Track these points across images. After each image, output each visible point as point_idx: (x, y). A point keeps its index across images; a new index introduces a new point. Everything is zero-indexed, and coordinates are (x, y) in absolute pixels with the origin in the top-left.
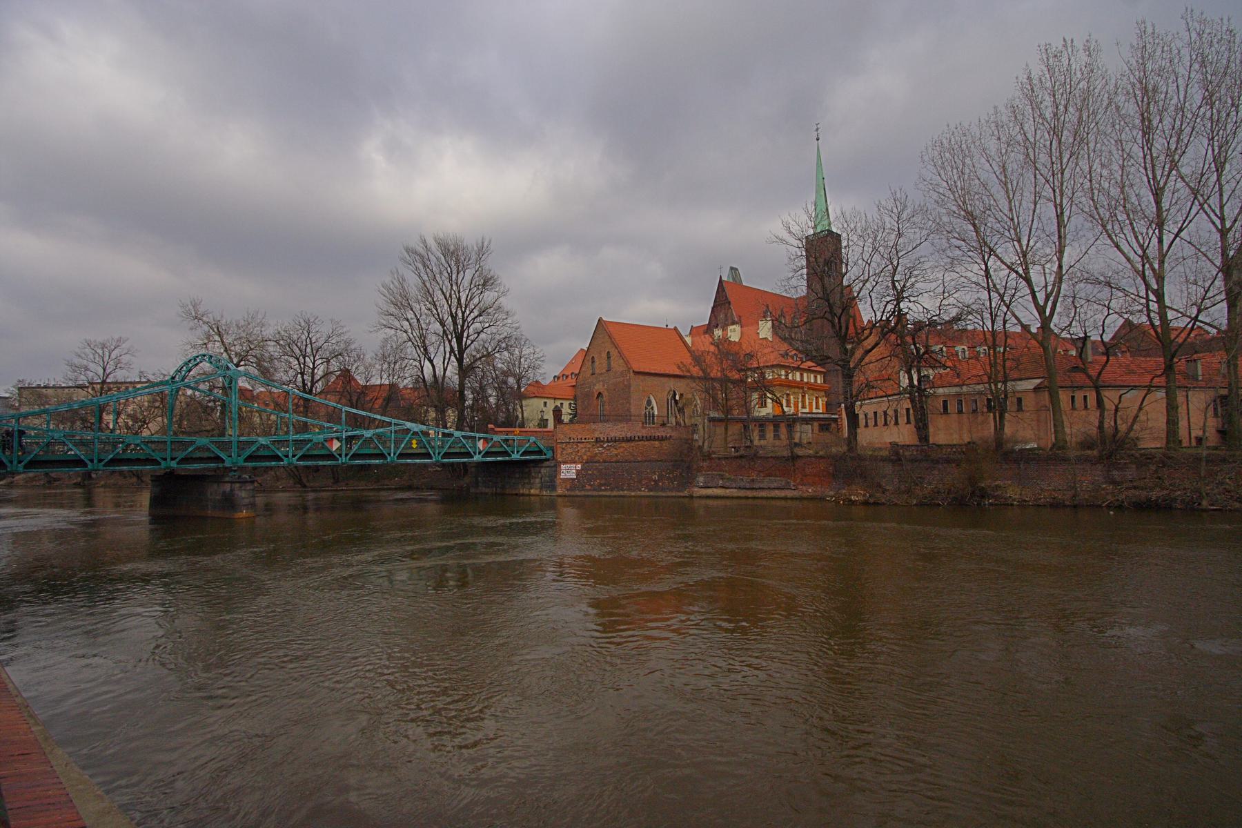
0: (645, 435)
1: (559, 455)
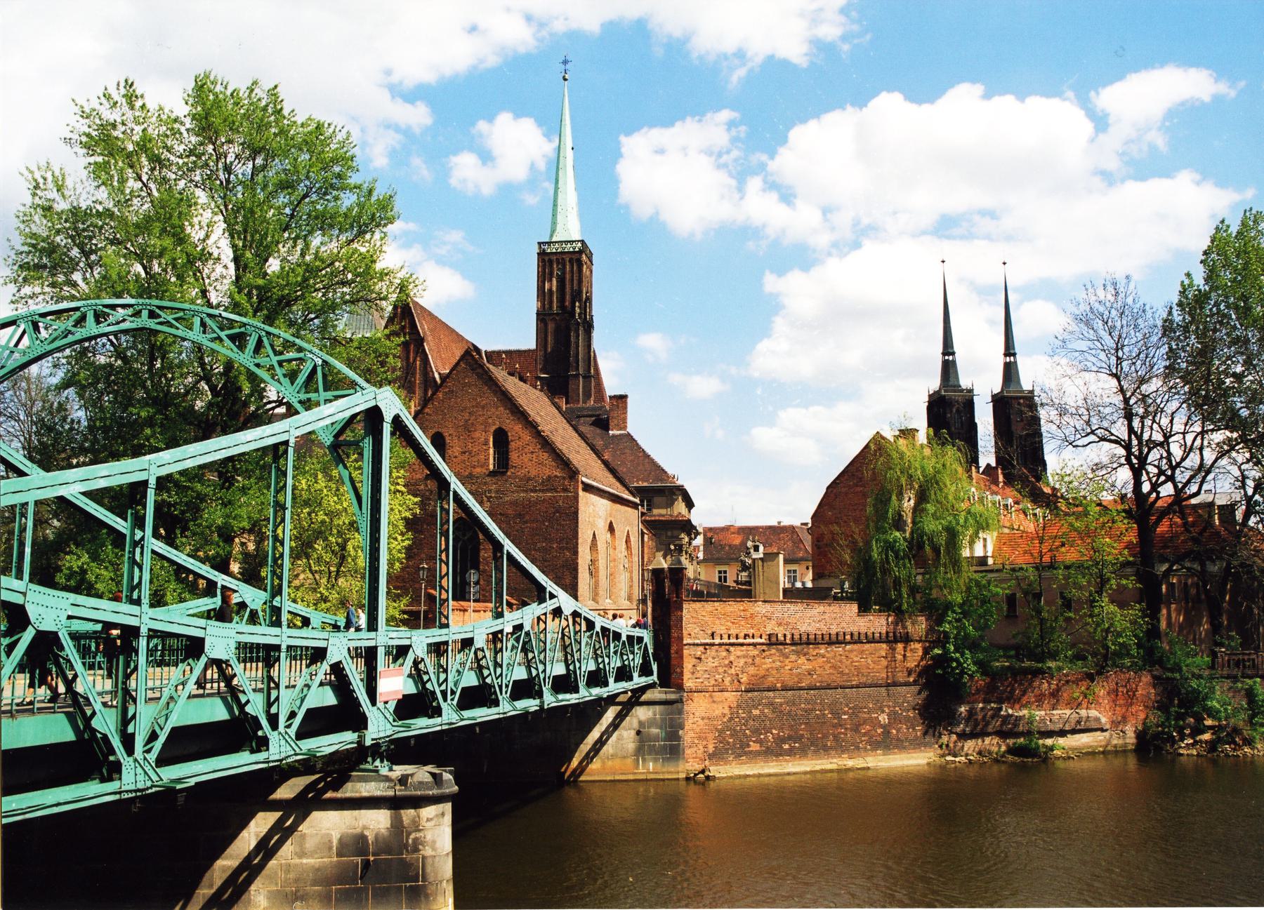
0: (863, 630)
1: (687, 675)
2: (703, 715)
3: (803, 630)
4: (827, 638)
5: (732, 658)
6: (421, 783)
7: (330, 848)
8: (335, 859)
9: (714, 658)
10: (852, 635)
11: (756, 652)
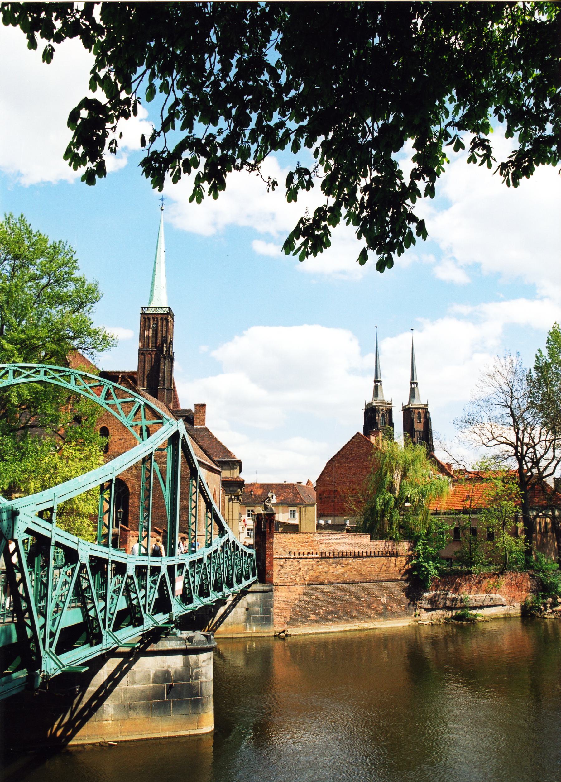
0: (373, 550)
2: (284, 599)
3: (339, 550)
4: (353, 554)
5: (301, 566)
6: (200, 641)
7: (149, 679)
8: (152, 685)
9: (290, 566)
10: (367, 552)
11: (314, 563)
